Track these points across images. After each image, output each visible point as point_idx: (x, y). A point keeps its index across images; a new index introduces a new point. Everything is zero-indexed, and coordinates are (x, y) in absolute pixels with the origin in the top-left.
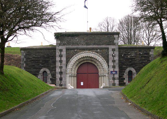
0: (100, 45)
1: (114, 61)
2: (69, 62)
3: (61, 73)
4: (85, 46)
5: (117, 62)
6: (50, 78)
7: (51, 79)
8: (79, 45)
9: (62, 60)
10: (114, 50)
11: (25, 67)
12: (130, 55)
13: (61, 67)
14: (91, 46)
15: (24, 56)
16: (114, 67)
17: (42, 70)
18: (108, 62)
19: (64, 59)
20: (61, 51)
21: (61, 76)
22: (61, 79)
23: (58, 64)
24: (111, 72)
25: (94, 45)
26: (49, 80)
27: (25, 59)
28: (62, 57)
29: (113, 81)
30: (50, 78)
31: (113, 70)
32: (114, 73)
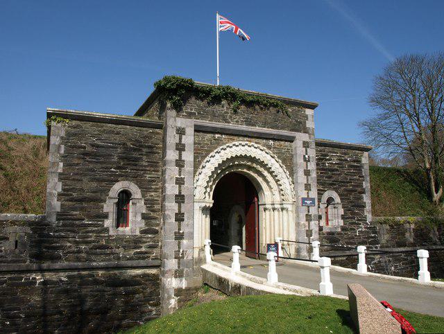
0: (277, 128)
1: (307, 173)
2: (201, 167)
3: (180, 198)
4: (244, 127)
5: (314, 175)
6: (143, 214)
7: (144, 217)
8: (229, 123)
9: (183, 159)
10: (306, 145)
11: (60, 174)
12: (329, 160)
13: (180, 182)
14: (257, 128)
15: (62, 138)
16: (308, 187)
17: (118, 187)
18: (292, 173)
19: (188, 156)
20: (181, 132)
21: (180, 207)
22: (180, 218)
23: (172, 172)
24: (303, 199)
25: (264, 127)
26: (139, 218)
27: (63, 146)
28: (184, 150)
29: (307, 224)
30: (143, 214)
31: (306, 197)
32: (308, 202)
